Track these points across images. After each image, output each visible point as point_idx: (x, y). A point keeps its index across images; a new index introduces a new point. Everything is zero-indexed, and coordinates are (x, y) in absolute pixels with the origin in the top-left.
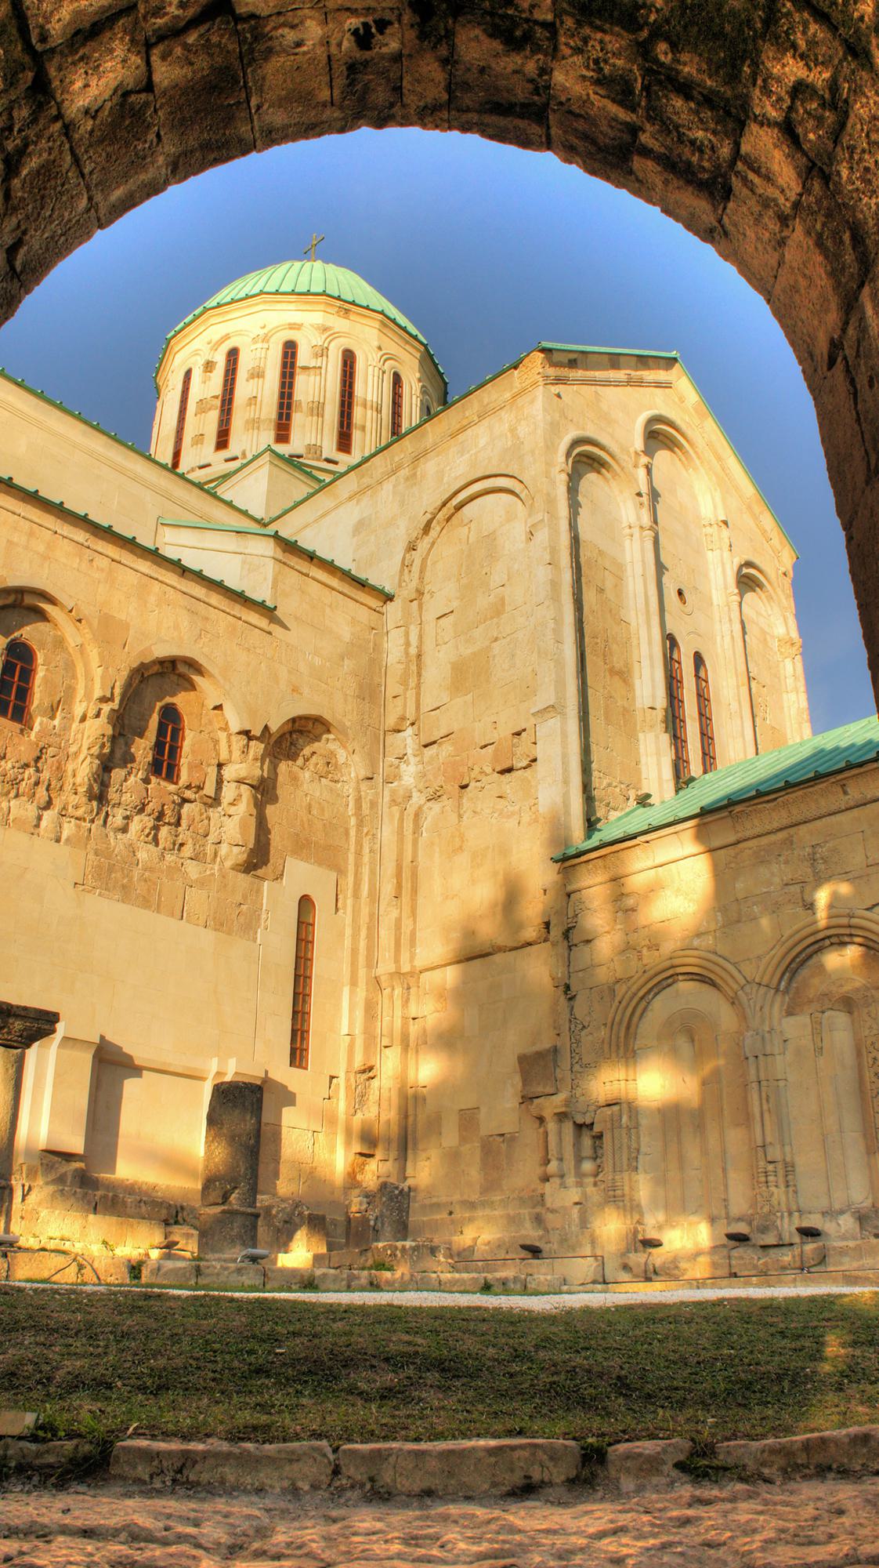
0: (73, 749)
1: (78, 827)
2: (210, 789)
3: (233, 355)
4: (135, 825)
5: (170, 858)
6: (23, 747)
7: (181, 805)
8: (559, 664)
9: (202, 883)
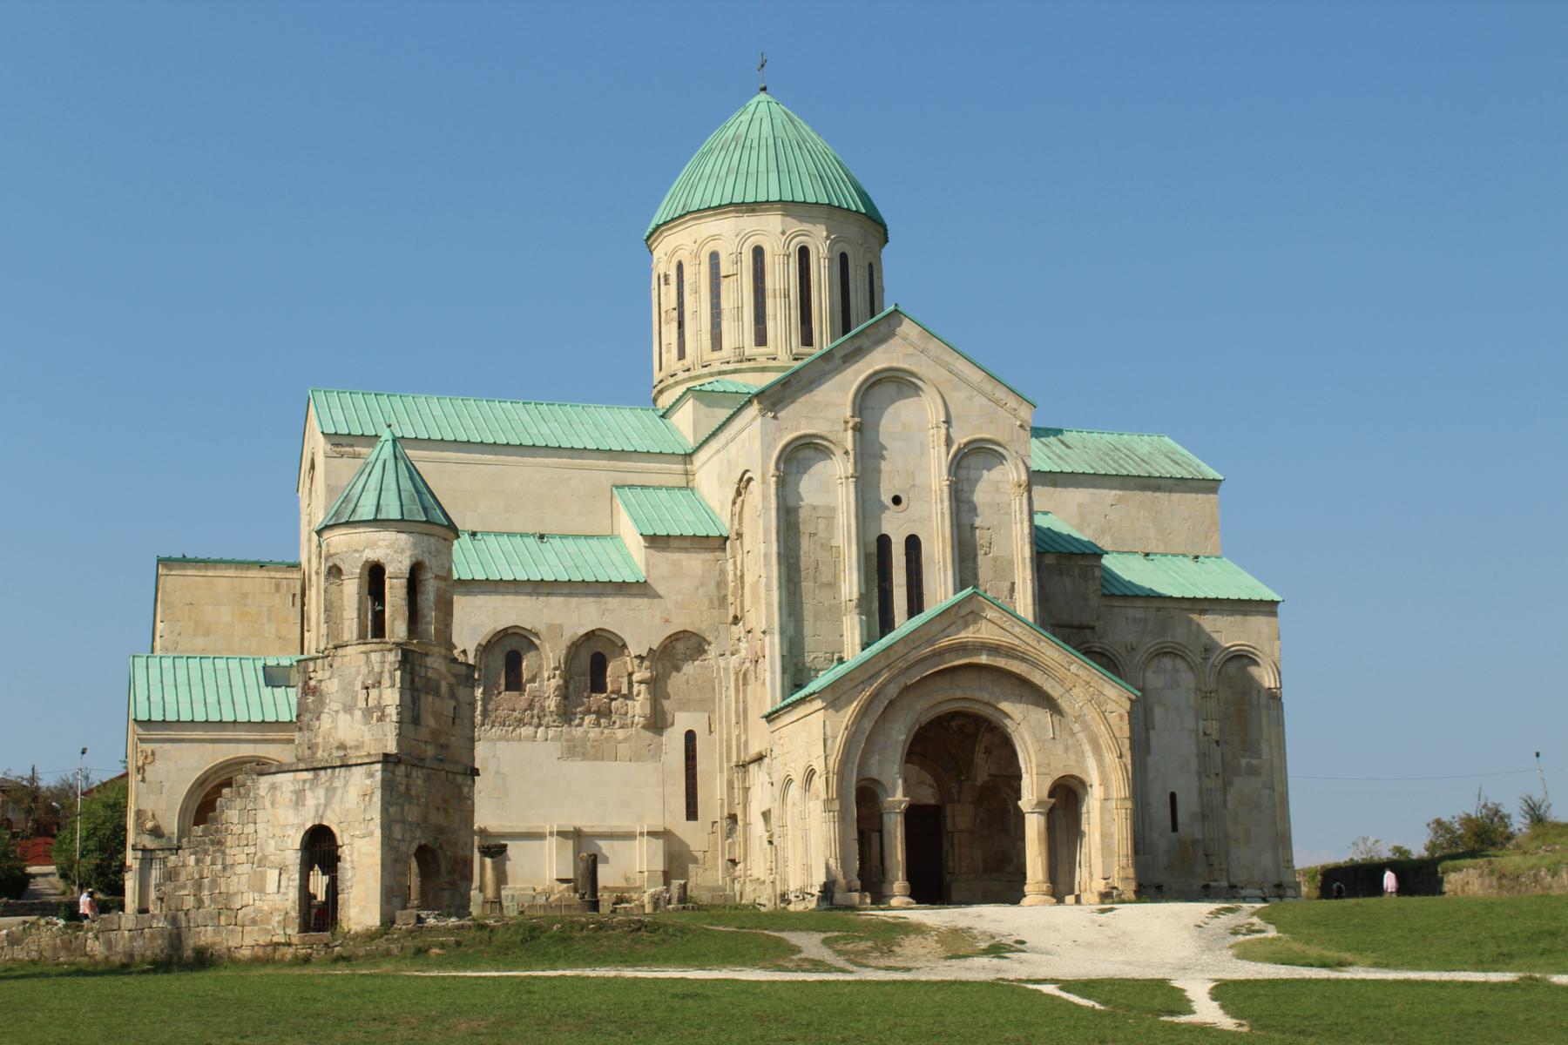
0: (546, 695)
1: (556, 731)
2: (625, 691)
3: (680, 266)
4: (587, 720)
5: (606, 731)
6: (523, 702)
7: (610, 703)
8: (769, 605)
9: (625, 740)
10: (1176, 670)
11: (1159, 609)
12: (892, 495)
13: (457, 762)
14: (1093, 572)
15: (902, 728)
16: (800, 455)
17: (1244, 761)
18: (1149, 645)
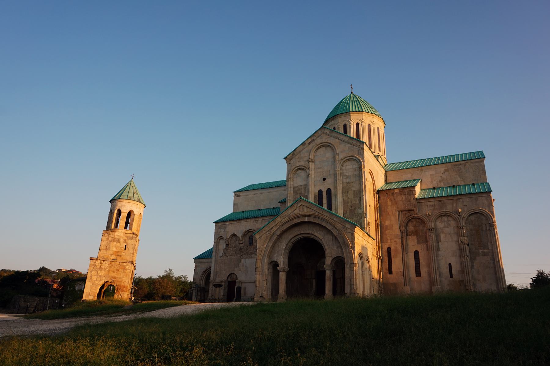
10: (450, 221)
11: (440, 201)
12: (323, 178)
13: (124, 260)
14: (413, 192)
15: (284, 244)
16: (298, 172)
17: (481, 251)
18: (436, 214)
